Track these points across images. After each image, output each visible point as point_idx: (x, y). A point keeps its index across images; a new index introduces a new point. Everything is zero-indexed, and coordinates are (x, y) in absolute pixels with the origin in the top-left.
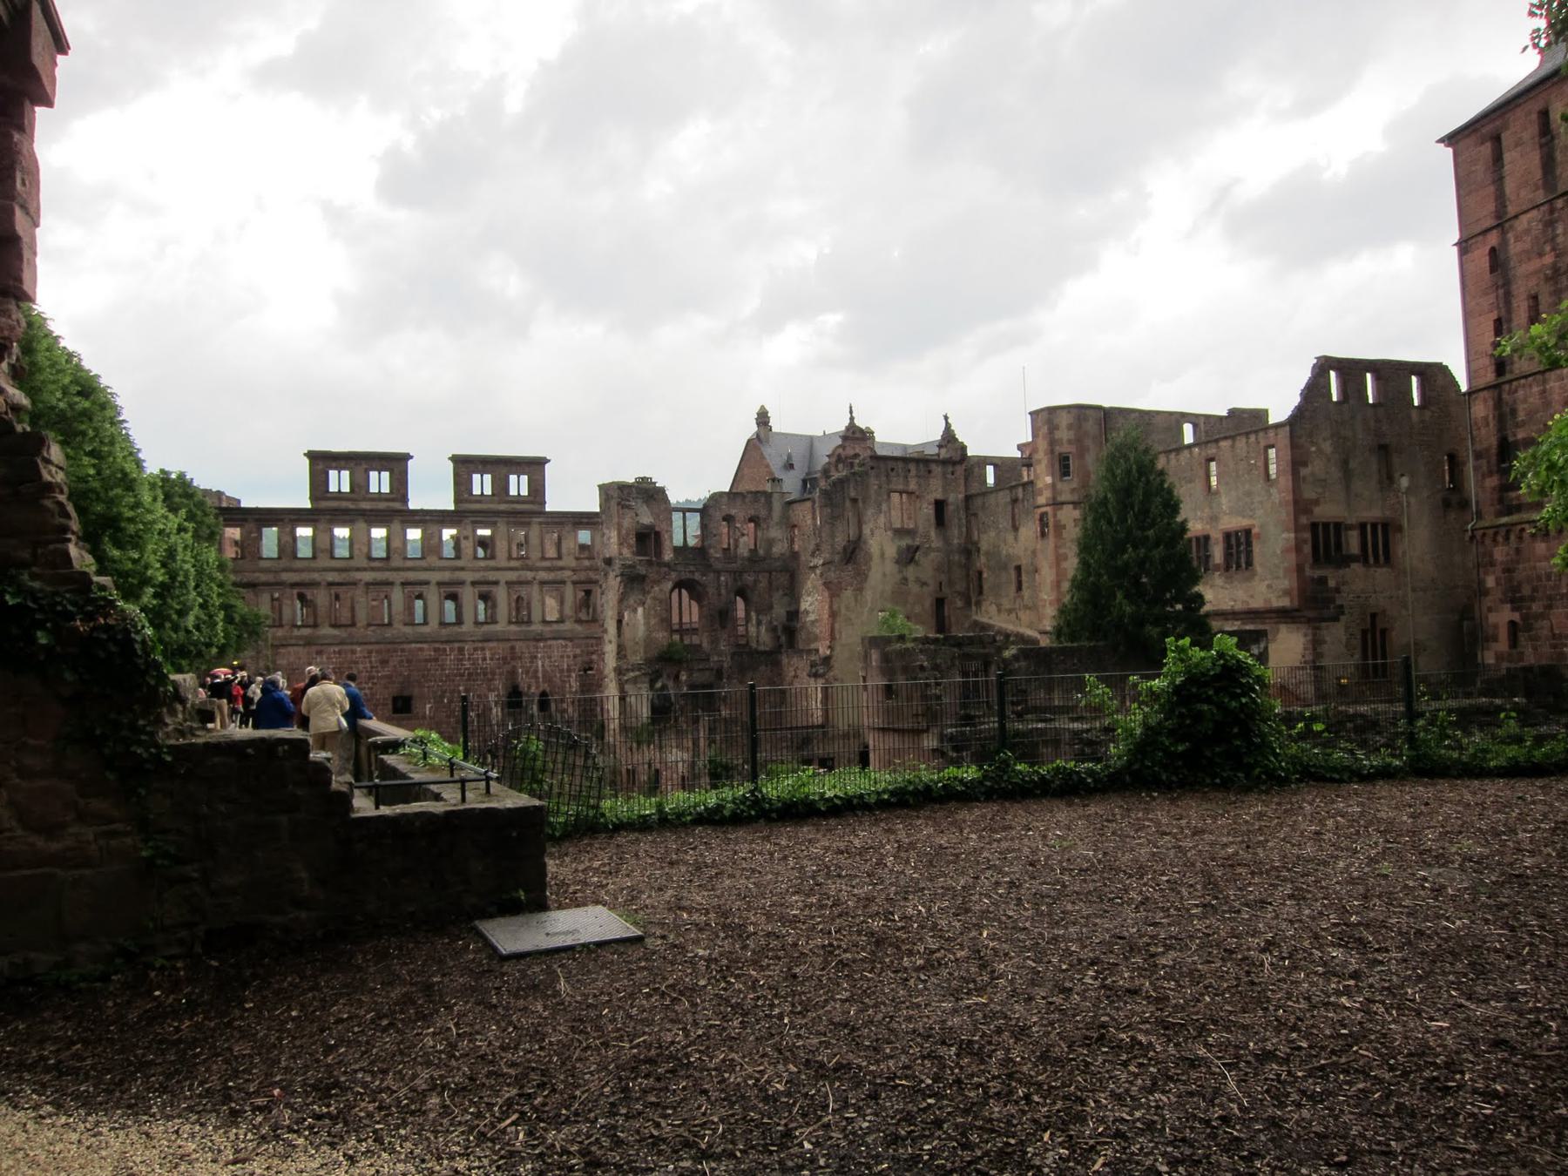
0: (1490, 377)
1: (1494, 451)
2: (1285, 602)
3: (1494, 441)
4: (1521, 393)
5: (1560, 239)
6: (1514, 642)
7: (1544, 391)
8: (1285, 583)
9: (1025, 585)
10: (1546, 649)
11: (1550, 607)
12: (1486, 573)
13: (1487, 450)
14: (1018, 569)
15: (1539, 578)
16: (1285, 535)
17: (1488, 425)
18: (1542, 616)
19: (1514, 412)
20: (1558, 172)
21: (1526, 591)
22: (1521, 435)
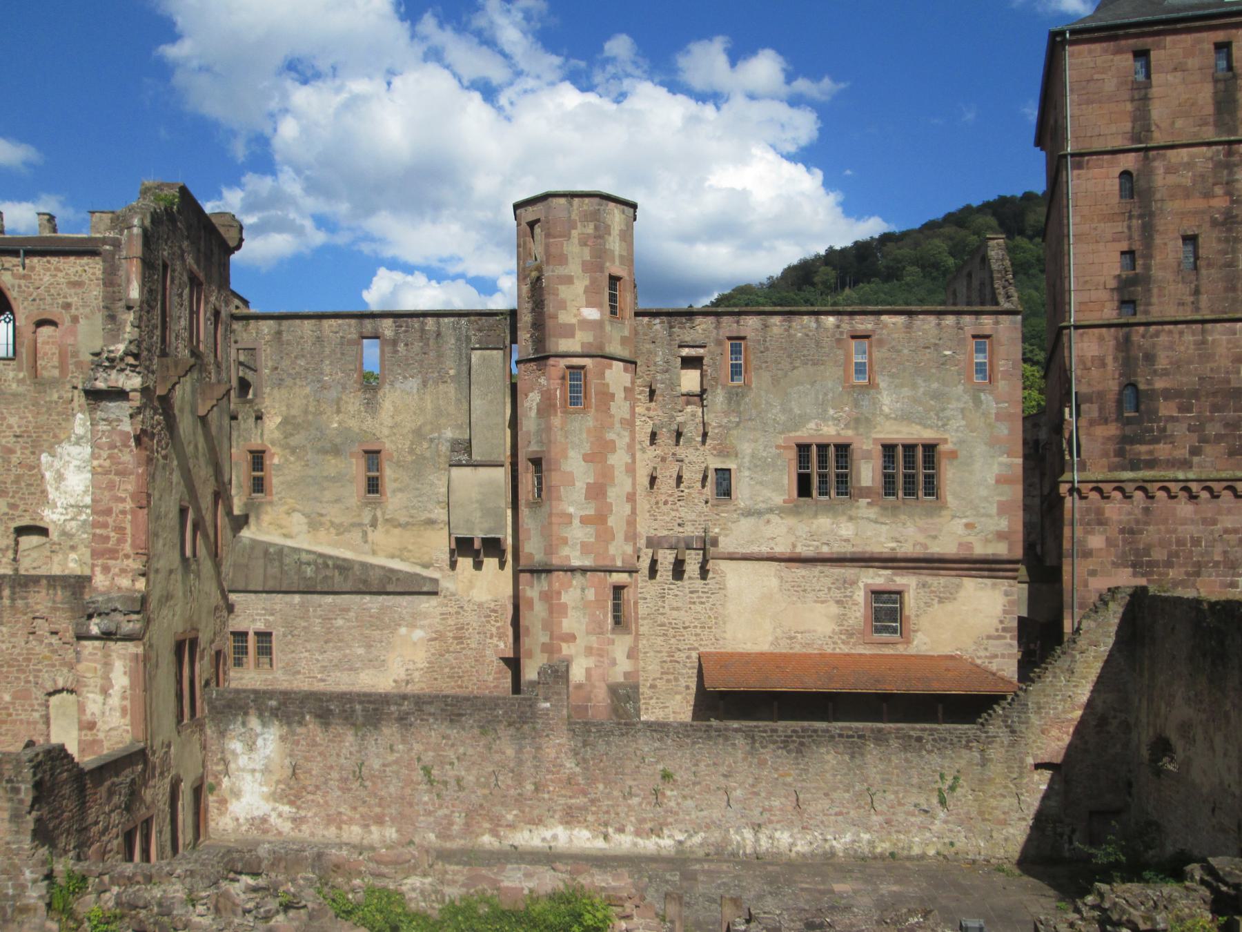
0: (1109, 312)
1: (1112, 397)
2: (1000, 549)
3: (1113, 386)
4: (1163, 339)
7: (1204, 342)
8: (1003, 524)
11: (1198, 574)
12: (1087, 533)
13: (1101, 395)
14: (373, 456)
15: (1180, 542)
17: (1103, 365)
19: (1150, 358)
21: (1159, 555)
22: (1160, 384)
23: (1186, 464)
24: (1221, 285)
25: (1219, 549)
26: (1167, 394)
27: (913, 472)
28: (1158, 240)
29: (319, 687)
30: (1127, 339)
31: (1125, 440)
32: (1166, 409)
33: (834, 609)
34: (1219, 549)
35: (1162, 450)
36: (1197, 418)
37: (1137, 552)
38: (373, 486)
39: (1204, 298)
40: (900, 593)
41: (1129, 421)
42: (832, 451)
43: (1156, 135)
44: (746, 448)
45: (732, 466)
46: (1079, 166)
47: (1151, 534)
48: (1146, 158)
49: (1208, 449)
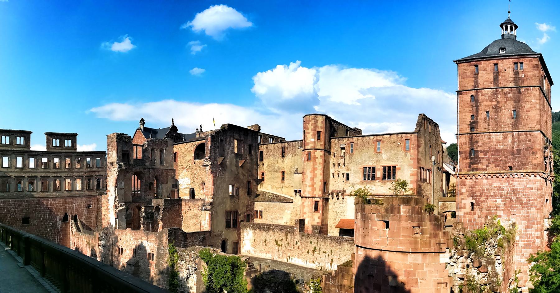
0: (468, 131)
1: (468, 152)
6: (472, 209)
9: (285, 179)
10: (485, 211)
11: (487, 199)
13: (465, 152)
15: (483, 190)
17: (466, 144)
18: (484, 201)
19: (477, 142)
21: (478, 194)
22: (479, 149)
23: (485, 169)
25: (493, 191)
26: (482, 151)
28: (480, 112)
29: (271, 223)
30: (472, 137)
31: (471, 163)
32: (481, 155)
35: (480, 166)
37: (473, 193)
38: (283, 179)
41: (472, 159)
47: (477, 188)
49: (491, 165)
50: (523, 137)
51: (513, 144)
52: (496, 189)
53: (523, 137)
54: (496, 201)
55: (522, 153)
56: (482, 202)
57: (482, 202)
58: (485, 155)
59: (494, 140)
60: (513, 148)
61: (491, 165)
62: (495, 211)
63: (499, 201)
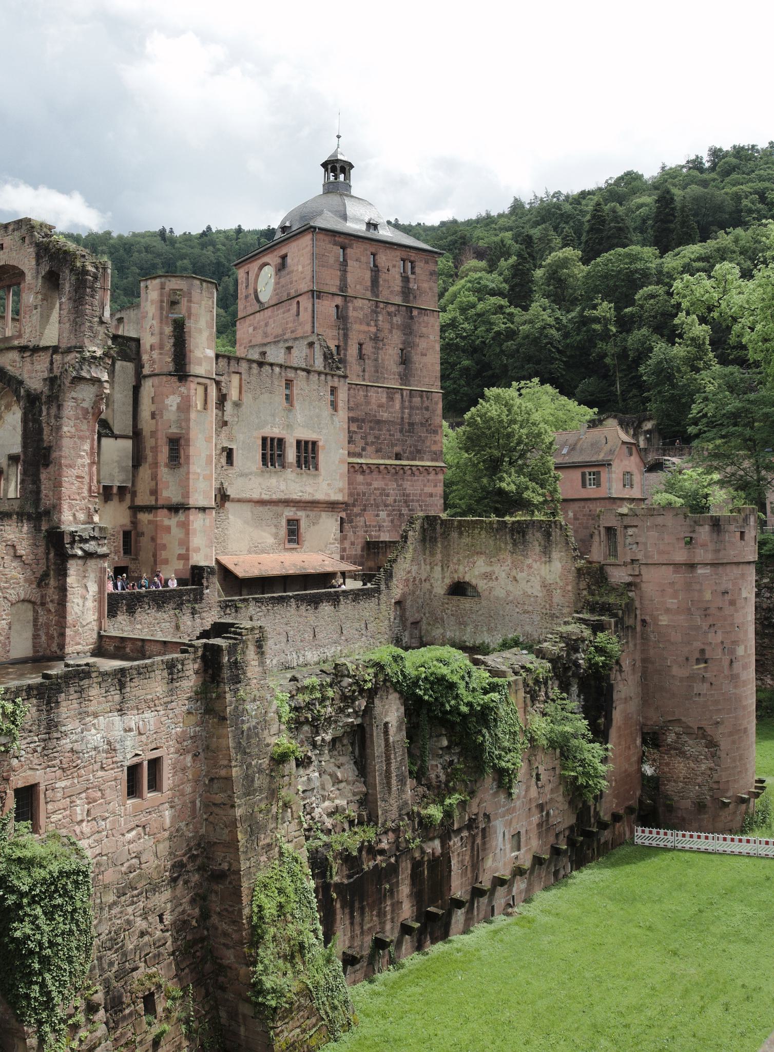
5: (380, 323)
7: (367, 396)
10: (361, 533)
11: (365, 510)
15: (358, 494)
16: (341, 451)
18: (360, 515)
20: (380, 289)
23: (360, 455)
24: (373, 369)
27: (308, 453)
33: (274, 530)
34: (372, 498)
36: (364, 433)
39: (367, 374)
40: (297, 520)
42: (276, 441)
43: (349, 290)
44: (241, 437)
45: (234, 446)
46: (318, 297)
48: (345, 300)
49: (368, 448)
50: (417, 400)
51: (403, 413)
52: (378, 492)
53: (417, 400)
54: (378, 515)
55: (415, 431)
56: (356, 515)
57: (356, 515)
58: (360, 428)
59: (373, 401)
60: (402, 418)
61: (368, 448)
62: (377, 534)
63: (383, 514)
